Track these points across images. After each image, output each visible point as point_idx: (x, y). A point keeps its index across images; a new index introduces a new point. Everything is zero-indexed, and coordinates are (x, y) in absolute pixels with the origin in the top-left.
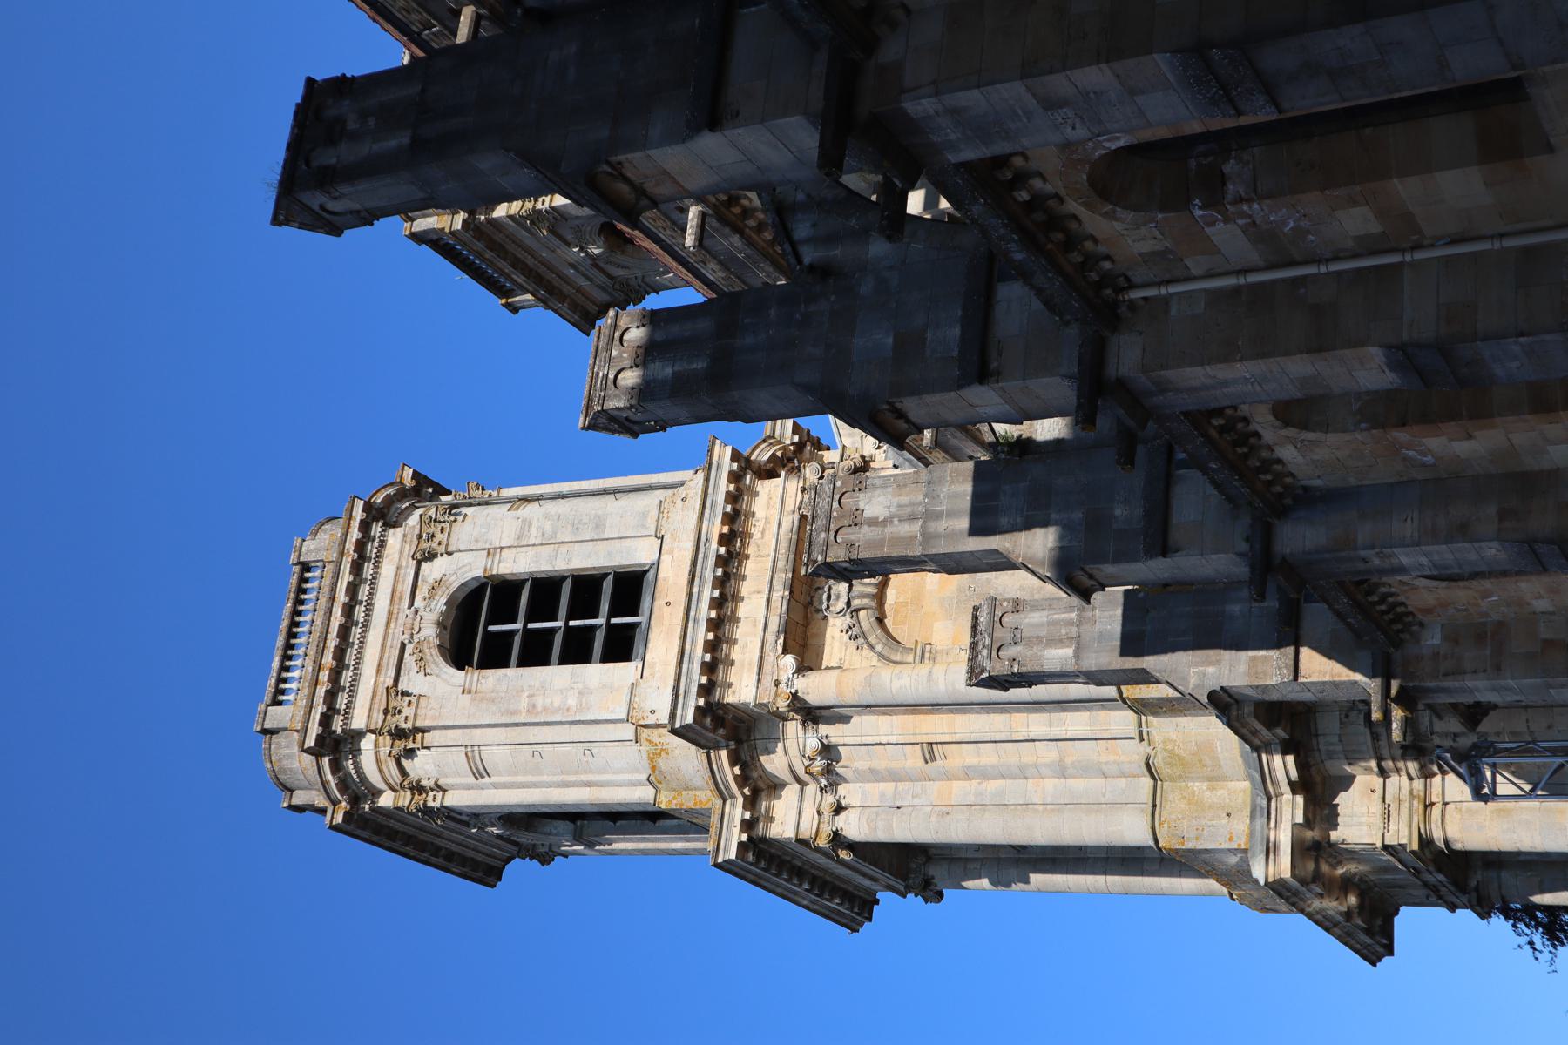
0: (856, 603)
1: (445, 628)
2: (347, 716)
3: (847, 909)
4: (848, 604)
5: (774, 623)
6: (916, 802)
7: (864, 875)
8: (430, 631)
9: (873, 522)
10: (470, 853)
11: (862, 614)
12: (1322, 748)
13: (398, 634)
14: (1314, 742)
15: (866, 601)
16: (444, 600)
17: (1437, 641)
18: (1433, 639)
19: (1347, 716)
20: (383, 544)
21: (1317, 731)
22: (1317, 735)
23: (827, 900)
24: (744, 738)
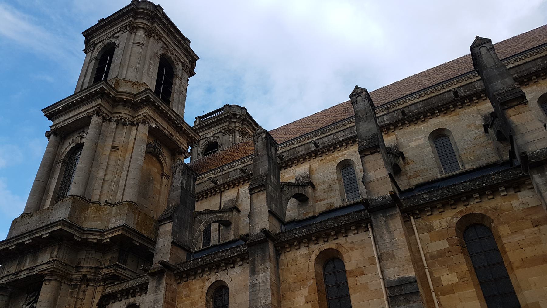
0: (156, 150)
1: (168, 58)
2: (158, 25)
3: (56, 110)
4: (157, 147)
5: (160, 127)
6: (100, 138)
7: (73, 117)
8: (170, 54)
9: (271, 149)
10: (99, 32)
11: (153, 150)
12: (91, 252)
13: (171, 48)
14: (94, 250)
15: (156, 152)
16: (174, 62)
17: (174, 286)
18: (174, 286)
19: (99, 262)
20: (187, 58)
21: (97, 252)
22: (96, 251)
23: (64, 106)
24: (132, 106)
